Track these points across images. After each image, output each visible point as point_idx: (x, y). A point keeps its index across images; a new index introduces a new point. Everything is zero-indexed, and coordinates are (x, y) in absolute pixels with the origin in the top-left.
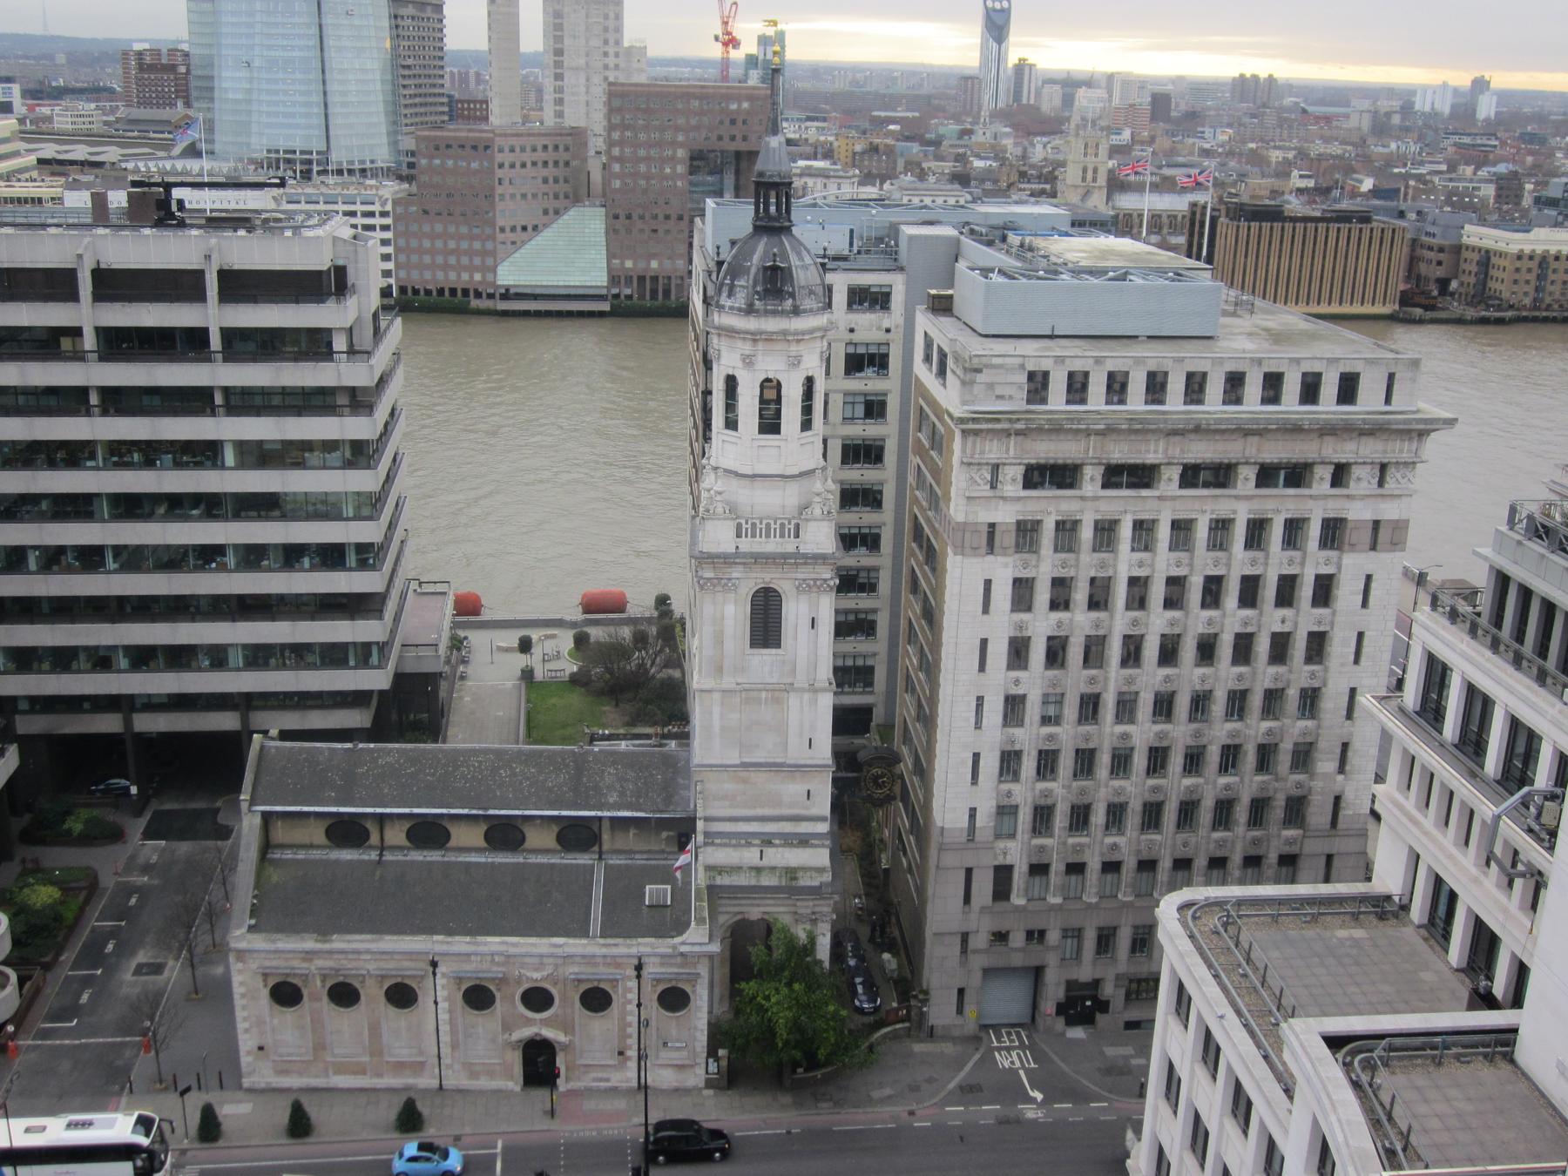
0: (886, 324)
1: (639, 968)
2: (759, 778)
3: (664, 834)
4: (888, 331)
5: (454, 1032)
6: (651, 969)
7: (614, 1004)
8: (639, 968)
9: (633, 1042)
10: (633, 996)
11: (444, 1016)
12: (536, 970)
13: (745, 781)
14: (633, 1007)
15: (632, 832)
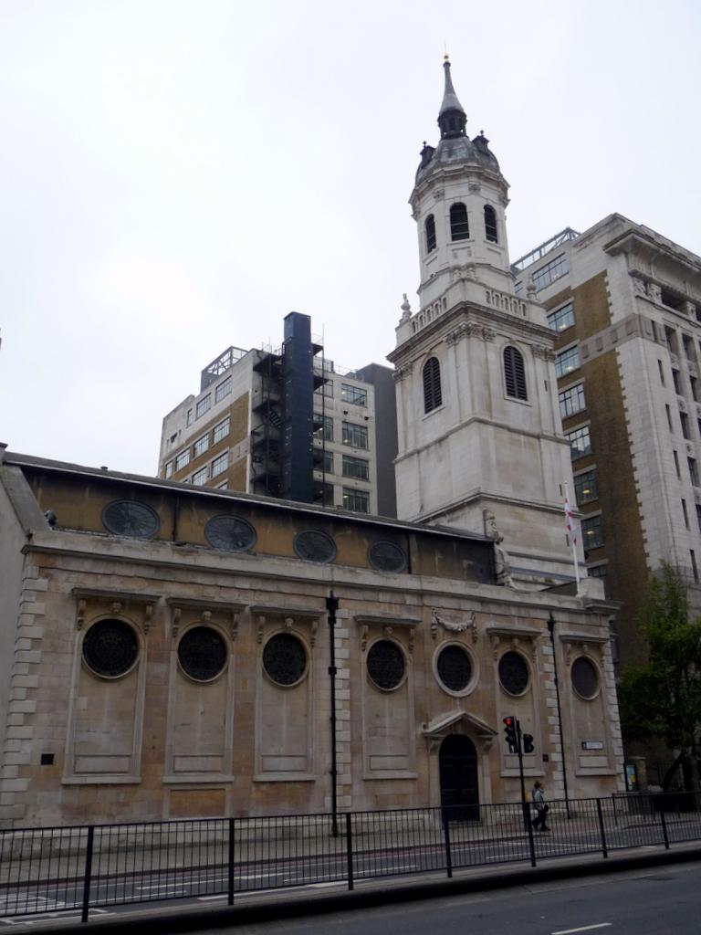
0: (365, 414)
1: (551, 625)
2: (531, 515)
3: (466, 563)
4: (367, 418)
5: (354, 722)
6: (561, 630)
7: (532, 680)
8: (551, 625)
9: (555, 738)
10: (549, 667)
11: (342, 694)
12: (454, 619)
13: (521, 518)
14: (550, 684)
15: (438, 557)
